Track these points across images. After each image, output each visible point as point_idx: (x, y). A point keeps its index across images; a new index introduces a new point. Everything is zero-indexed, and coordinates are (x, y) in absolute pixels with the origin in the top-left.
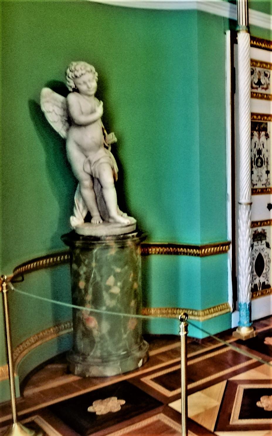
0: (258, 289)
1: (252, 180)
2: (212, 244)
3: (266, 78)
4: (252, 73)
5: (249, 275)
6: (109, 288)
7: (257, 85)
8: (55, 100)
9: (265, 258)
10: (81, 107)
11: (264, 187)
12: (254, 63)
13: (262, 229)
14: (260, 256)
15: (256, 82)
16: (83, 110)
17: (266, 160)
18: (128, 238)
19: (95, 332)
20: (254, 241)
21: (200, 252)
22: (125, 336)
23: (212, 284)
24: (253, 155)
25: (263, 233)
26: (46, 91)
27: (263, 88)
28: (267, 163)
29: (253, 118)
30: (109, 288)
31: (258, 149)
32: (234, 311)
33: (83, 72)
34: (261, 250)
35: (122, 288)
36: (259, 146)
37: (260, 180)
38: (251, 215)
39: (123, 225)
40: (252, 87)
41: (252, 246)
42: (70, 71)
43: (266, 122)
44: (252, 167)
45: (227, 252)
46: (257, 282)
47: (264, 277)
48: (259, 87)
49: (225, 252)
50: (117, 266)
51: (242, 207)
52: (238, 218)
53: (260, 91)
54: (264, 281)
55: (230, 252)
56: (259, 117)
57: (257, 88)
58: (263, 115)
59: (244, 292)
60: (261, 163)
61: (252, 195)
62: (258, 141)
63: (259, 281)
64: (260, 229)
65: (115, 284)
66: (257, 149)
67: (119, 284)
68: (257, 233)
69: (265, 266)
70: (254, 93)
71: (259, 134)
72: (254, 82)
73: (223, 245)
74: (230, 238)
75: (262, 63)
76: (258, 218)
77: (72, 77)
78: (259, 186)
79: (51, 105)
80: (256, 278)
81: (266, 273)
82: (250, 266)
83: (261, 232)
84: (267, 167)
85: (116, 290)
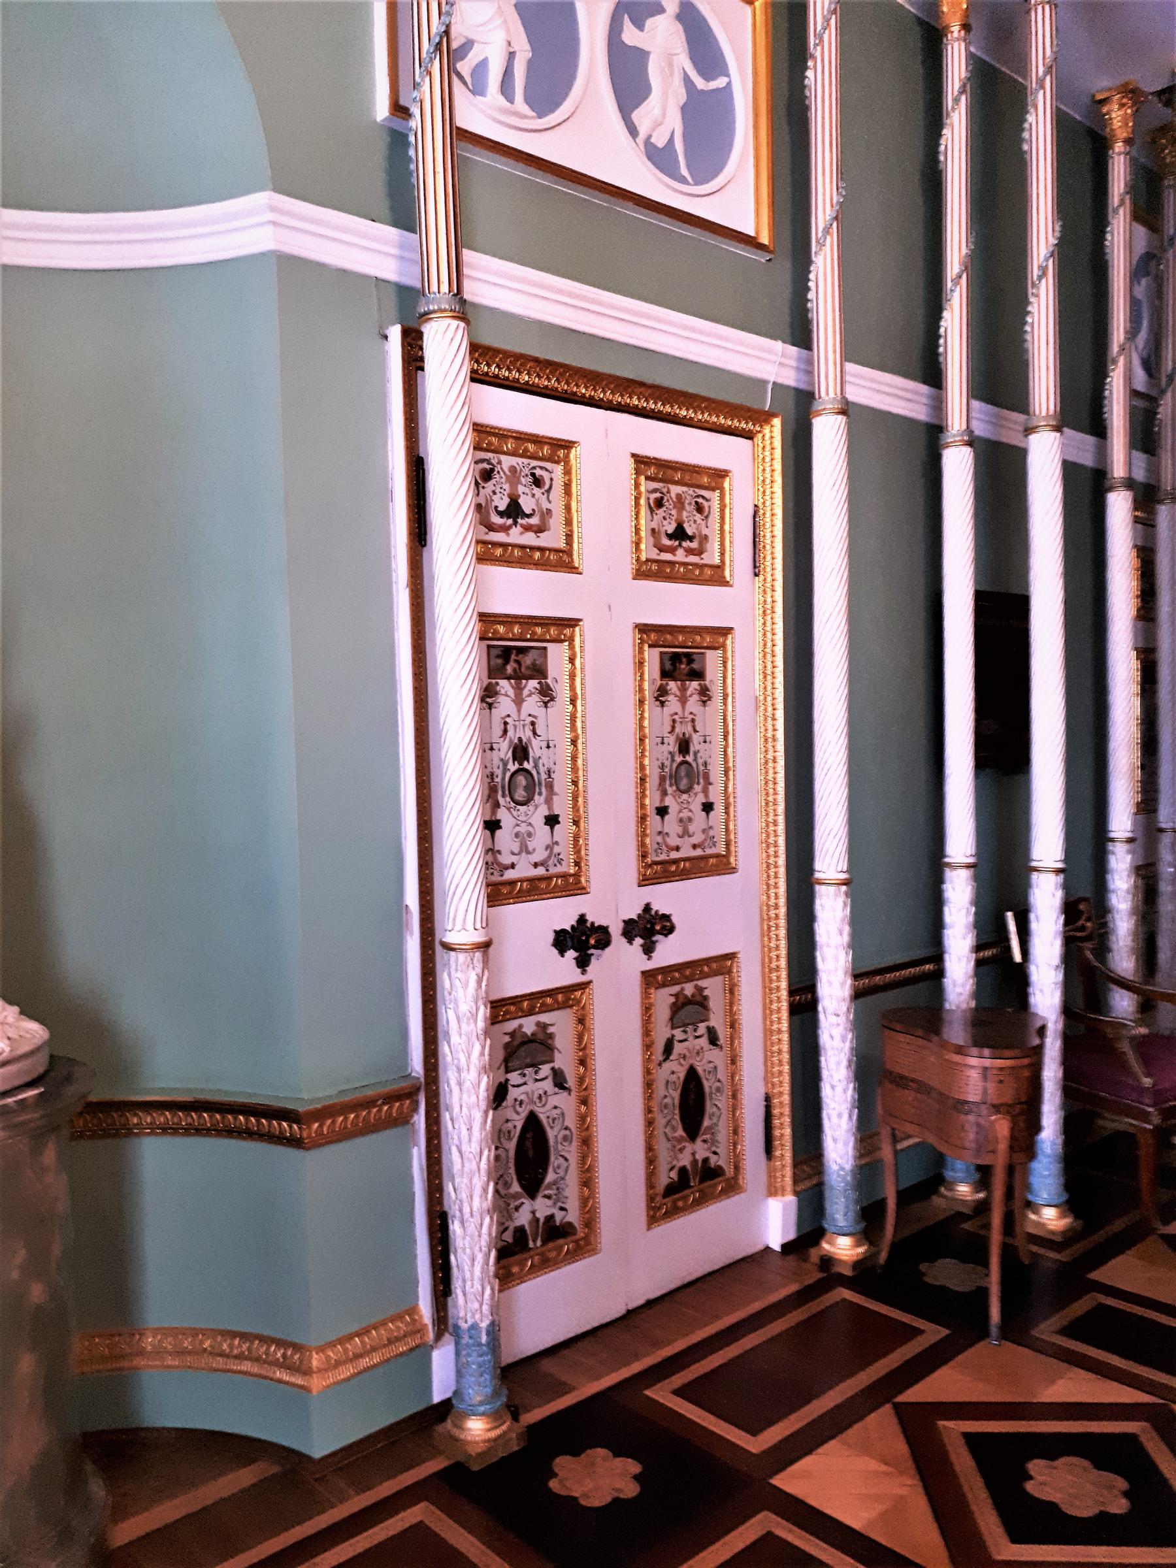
0: (531, 1244)
2: (347, 1098)
3: (536, 490)
5: (487, 1220)
7: (509, 517)
9: (552, 1127)
11: (541, 871)
12: (486, 438)
13: (538, 1024)
14: (533, 1123)
15: (502, 508)
17: (544, 776)
25: (541, 1036)
27: (527, 528)
28: (550, 786)
36: (520, 734)
37: (525, 849)
43: (544, 644)
46: (523, 1218)
47: (548, 1197)
48: (515, 523)
49: (404, 1120)
53: (516, 536)
54: (548, 1213)
55: (420, 1119)
57: (505, 529)
58: (529, 621)
59: (469, 1283)
60: (526, 788)
62: (515, 716)
63: (533, 1212)
64: (528, 1025)
69: (552, 1158)
71: (519, 689)
72: (496, 507)
73: (390, 1098)
75: (522, 437)
76: (516, 985)
78: (524, 870)
81: (555, 1183)
82: (488, 1185)
84: (549, 802)
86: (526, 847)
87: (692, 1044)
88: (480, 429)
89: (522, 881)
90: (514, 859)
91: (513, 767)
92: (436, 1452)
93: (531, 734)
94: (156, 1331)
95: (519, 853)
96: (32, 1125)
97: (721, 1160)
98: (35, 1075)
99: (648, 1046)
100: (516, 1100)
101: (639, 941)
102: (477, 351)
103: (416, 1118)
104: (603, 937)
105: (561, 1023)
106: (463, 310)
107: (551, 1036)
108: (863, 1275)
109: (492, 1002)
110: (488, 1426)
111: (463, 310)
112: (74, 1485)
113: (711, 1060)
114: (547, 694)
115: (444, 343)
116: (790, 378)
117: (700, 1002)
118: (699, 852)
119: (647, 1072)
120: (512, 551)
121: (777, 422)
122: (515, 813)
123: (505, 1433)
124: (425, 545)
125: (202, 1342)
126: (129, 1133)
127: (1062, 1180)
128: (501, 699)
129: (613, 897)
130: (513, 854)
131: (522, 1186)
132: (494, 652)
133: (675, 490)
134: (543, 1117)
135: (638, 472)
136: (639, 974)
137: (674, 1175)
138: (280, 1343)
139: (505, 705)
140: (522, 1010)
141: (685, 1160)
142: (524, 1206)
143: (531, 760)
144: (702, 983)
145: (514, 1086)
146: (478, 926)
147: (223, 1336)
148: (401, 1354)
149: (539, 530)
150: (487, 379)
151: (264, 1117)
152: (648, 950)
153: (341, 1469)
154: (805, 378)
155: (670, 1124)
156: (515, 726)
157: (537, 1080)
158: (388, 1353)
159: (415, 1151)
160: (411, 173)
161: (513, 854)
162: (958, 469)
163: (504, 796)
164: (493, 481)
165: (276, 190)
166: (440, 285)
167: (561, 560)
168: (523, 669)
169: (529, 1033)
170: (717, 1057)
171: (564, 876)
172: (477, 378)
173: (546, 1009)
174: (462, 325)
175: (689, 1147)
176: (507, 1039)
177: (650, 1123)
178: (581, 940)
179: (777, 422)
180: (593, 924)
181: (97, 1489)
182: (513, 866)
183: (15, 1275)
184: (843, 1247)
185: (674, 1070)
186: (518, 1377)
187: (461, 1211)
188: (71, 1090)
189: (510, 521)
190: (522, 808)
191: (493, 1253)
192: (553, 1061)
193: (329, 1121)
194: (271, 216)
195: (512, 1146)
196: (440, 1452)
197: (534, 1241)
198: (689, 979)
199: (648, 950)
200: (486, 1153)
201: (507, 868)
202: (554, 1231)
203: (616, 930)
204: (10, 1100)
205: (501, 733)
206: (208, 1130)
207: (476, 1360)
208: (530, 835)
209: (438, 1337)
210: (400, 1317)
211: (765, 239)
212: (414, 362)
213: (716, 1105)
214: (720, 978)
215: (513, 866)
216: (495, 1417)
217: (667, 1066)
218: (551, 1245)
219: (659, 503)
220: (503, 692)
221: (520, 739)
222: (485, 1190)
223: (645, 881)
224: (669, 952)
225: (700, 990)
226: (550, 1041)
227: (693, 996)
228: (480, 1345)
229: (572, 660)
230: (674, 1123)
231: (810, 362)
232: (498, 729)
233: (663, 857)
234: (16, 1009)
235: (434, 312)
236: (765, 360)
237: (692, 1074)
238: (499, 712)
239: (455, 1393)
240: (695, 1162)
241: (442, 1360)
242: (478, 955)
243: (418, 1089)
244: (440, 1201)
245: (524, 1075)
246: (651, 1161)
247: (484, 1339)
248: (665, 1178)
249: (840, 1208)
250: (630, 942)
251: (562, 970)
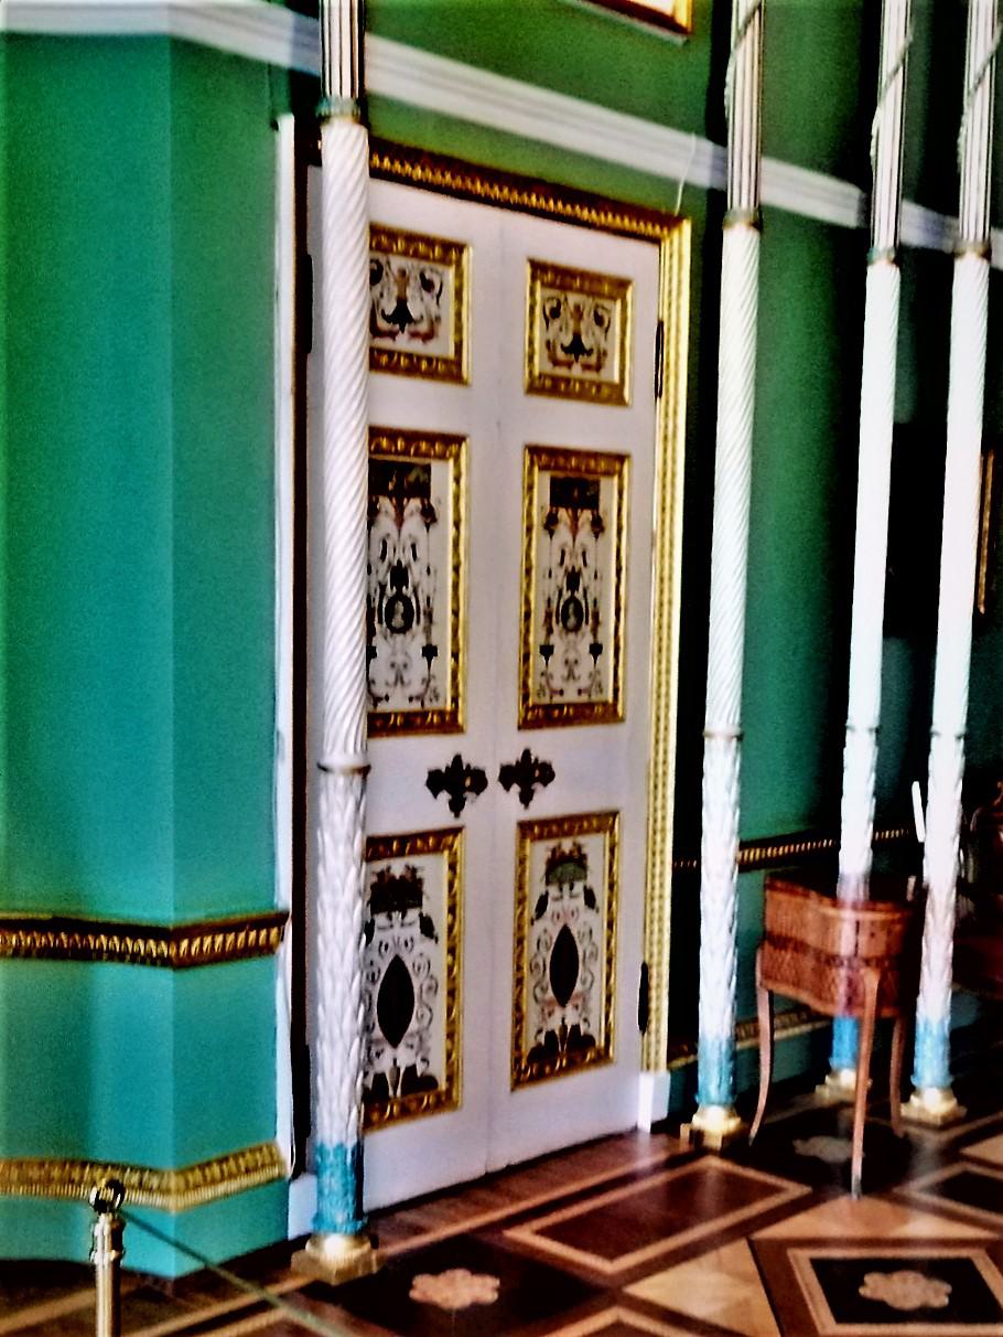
0: (391, 1093)
1: (369, 682)
4: (376, 276)
5: (357, 1041)
7: (395, 323)
9: (417, 975)
11: (416, 706)
12: (381, 238)
13: (407, 867)
14: (397, 966)
17: (423, 605)
20: (375, 911)
21: (173, 952)
24: (374, 585)
27: (414, 335)
28: (429, 615)
31: (395, 563)
34: (403, 947)
36: (399, 554)
37: (399, 679)
40: (375, 331)
41: (368, 929)
43: (427, 461)
44: (371, 633)
45: (274, 953)
46: (384, 1065)
47: (412, 1047)
49: (268, 950)
52: (317, 823)
53: (403, 343)
54: (410, 1063)
55: (286, 951)
56: (400, 444)
58: (413, 437)
59: (335, 1104)
60: (404, 616)
62: (394, 534)
64: (398, 867)
66: (390, 564)
69: (416, 1004)
70: (381, 351)
71: (400, 509)
72: (383, 312)
74: (284, 899)
75: (411, 238)
78: (398, 703)
82: (359, 1006)
84: (428, 631)
86: (402, 678)
87: (567, 903)
88: (375, 231)
97: (595, 1029)
99: (521, 901)
101: (516, 789)
104: (479, 781)
105: (432, 869)
107: (420, 881)
108: (734, 1147)
111: (365, 106)
113: (586, 924)
114: (429, 516)
115: (343, 143)
116: (703, 178)
117: (579, 860)
118: (584, 698)
119: (520, 928)
121: (687, 227)
127: (947, 1063)
129: (491, 739)
133: (573, 299)
134: (409, 965)
135: (534, 278)
136: (515, 826)
137: (542, 1038)
139: (386, 523)
141: (554, 1024)
144: (582, 840)
149: (428, 336)
152: (526, 798)
154: (719, 176)
155: (539, 985)
162: (883, 287)
167: (450, 371)
170: (597, 920)
171: (441, 713)
173: (414, 851)
175: (558, 1013)
177: (519, 982)
178: (456, 782)
179: (687, 227)
180: (468, 766)
184: (714, 1121)
185: (548, 928)
187: (331, 1031)
198: (569, 834)
199: (526, 798)
202: (417, 1083)
203: (493, 775)
209: (295, 1176)
211: (683, 18)
212: (308, 154)
213: (591, 974)
214: (601, 836)
217: (540, 925)
218: (411, 1096)
219: (555, 313)
223: (525, 725)
224: (549, 802)
225: (579, 848)
227: (571, 852)
229: (457, 480)
230: (544, 984)
231: (725, 159)
233: (546, 700)
236: (677, 157)
237: (565, 934)
240: (564, 1027)
241: (301, 1197)
246: (519, 1019)
248: (530, 1042)
249: (713, 1079)
250: (507, 787)
251: (434, 813)
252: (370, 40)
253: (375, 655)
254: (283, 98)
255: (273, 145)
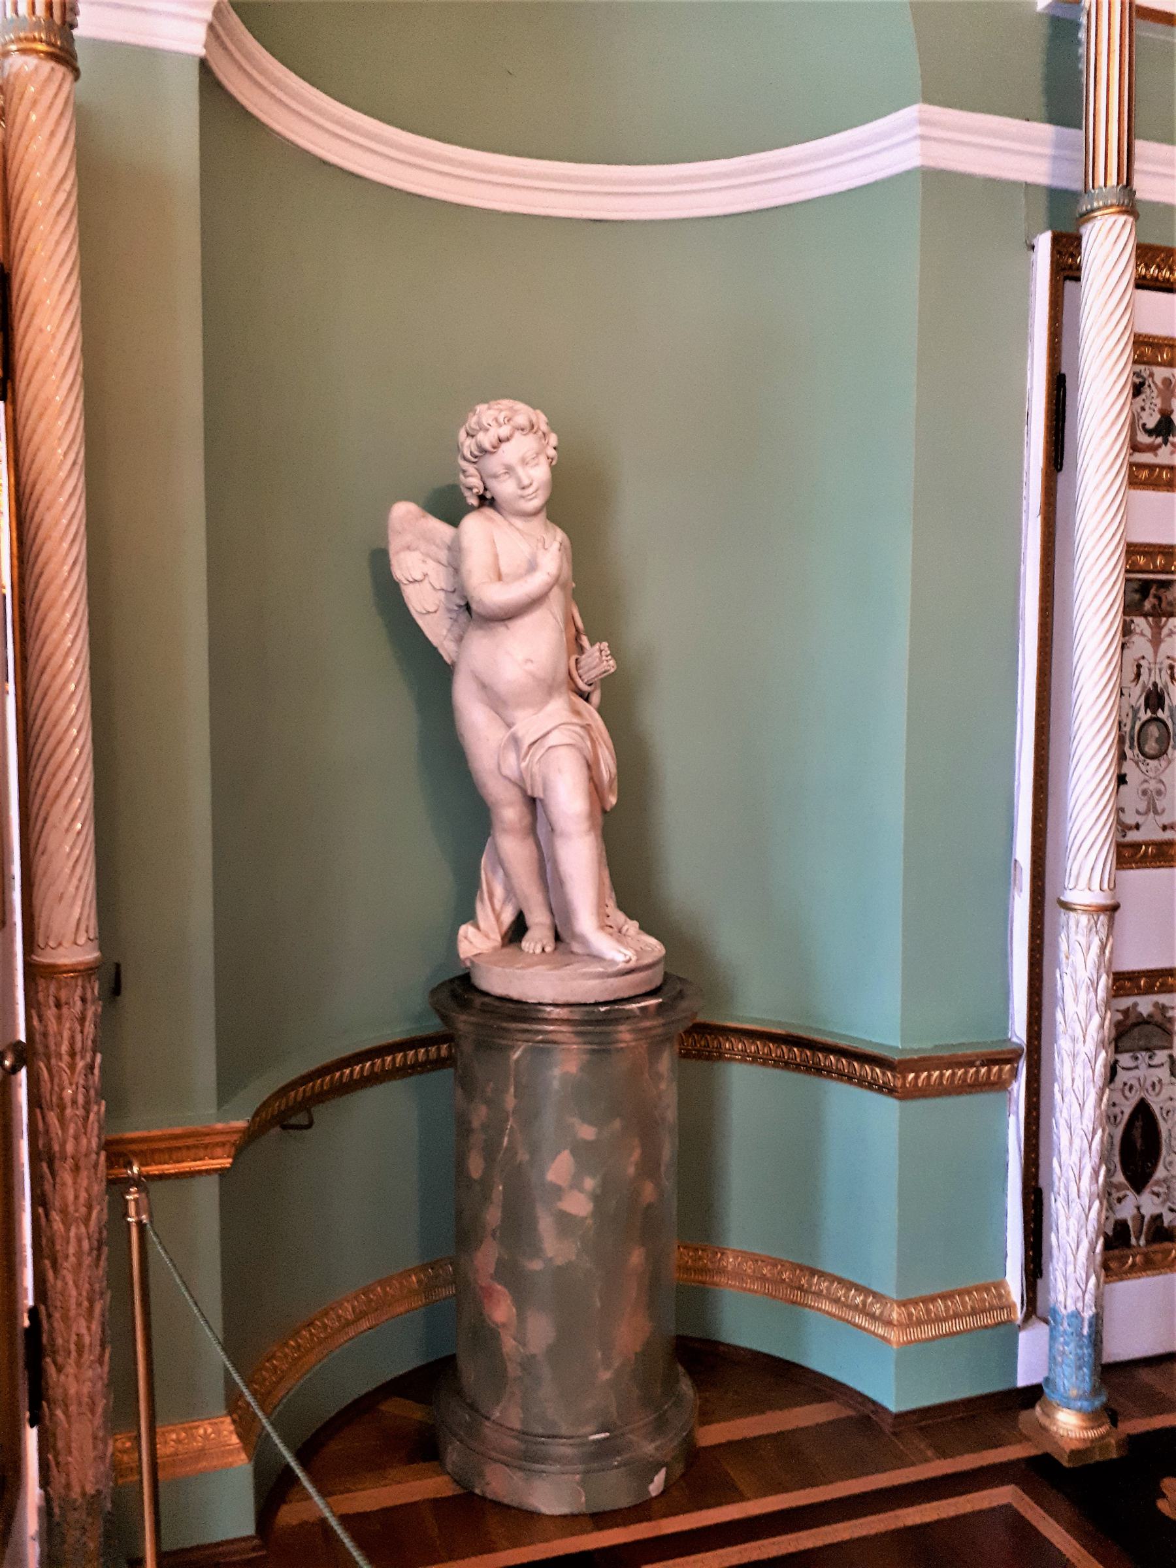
0: (1133, 1241)
1: (1120, 810)
2: (945, 1053)
4: (1137, 390)
6: (557, 1191)
8: (428, 539)
10: (496, 557)
14: (1143, 1111)
16: (504, 569)
18: (629, 1017)
19: (509, 1344)
20: (1117, 1051)
21: (899, 1083)
22: (606, 1376)
23: (943, 1208)
24: (1126, 709)
25: (1158, 1018)
26: (403, 511)
29: (1134, 563)
30: (557, 1191)
31: (1150, 686)
32: (1027, 1318)
33: (504, 431)
34: (1150, 1089)
35: (598, 1199)
38: (1111, 953)
39: (611, 970)
40: (1135, 447)
41: (1112, 1070)
42: (468, 434)
44: (1122, 757)
45: (1006, 1089)
46: (1126, 1212)
47: (1158, 1195)
49: (1000, 1085)
50: (585, 1119)
51: (1072, 923)
52: (1056, 963)
54: (1157, 1211)
55: (1019, 1088)
56: (1159, 561)
57: (1153, 449)
61: (1117, 869)
63: (1138, 1208)
65: (576, 1185)
66: (1144, 686)
67: (589, 1183)
68: (1132, 1019)
69: (1164, 1152)
70: (1141, 466)
72: (1144, 425)
73: (990, 1061)
74: (1019, 1032)
77: (471, 453)
79: (418, 557)
80: (1125, 1196)
81: (1165, 1180)
83: (1150, 1016)
85: (579, 1205)
89: (1147, 844)
90: (1140, 819)
91: (1144, 715)
92: (1023, 1438)
93: (1169, 680)
94: (737, 1253)
95: (1147, 813)
96: (654, 1032)
98: (653, 986)
100: (1125, 1084)
102: (1145, 253)
103: (1015, 1086)
106: (1130, 206)
109: (1115, 974)
110: (1084, 1425)
112: (670, 1382)
115: (1107, 245)
120: (1160, 474)
122: (1143, 768)
123: (1102, 1437)
124: (1061, 470)
125: (780, 1273)
126: (721, 1057)
128: (1135, 638)
130: (1138, 812)
131: (1127, 1178)
132: (1135, 585)
134: (1156, 1109)
138: (860, 1289)
139: (1141, 645)
140: (1139, 987)
142: (1128, 1199)
143: (1166, 708)
145: (1123, 1068)
146: (1105, 886)
147: (801, 1270)
148: (986, 1327)
150: (1158, 284)
151: (856, 1060)
153: (921, 1429)
156: (1150, 670)
157: (1150, 1066)
158: (970, 1322)
159: (1012, 1120)
160: (1078, 58)
161: (1138, 812)
163: (1131, 747)
164: (1143, 396)
165: (928, 99)
166: (1107, 177)
168: (1164, 605)
169: (1145, 1015)
172: (1142, 283)
174: (1131, 219)
176: (1120, 1017)
181: (686, 1386)
182: (1137, 827)
183: (631, 1170)
186: (1117, 1382)
188: (684, 1004)
189: (1159, 440)
190: (1153, 763)
191: (1101, 1241)
192: (1171, 1048)
193: (925, 1074)
194: (918, 130)
195: (1119, 1132)
196: (1028, 1439)
197: (1138, 1238)
200: (1100, 1132)
201: (1130, 828)
204: (634, 1006)
205: (1133, 676)
206: (798, 1065)
207: (1071, 1350)
208: (1159, 793)
210: (987, 1289)
212: (1067, 268)
215: (1137, 827)
216: (1093, 1417)
218: (1156, 1247)
220: (1138, 630)
221: (1155, 685)
222: (1096, 1173)
226: (1168, 1026)
228: (1081, 1335)
232: (1130, 672)
234: (636, 924)
235: (1099, 209)
238: (1132, 654)
239: (1047, 1379)
242: (1103, 918)
243: (1020, 1056)
244: (1036, 1177)
245: (1137, 1058)
247: (1086, 1331)
252: (1139, 146)
253: (1125, 782)
254: (1041, 214)
255: (1030, 266)
